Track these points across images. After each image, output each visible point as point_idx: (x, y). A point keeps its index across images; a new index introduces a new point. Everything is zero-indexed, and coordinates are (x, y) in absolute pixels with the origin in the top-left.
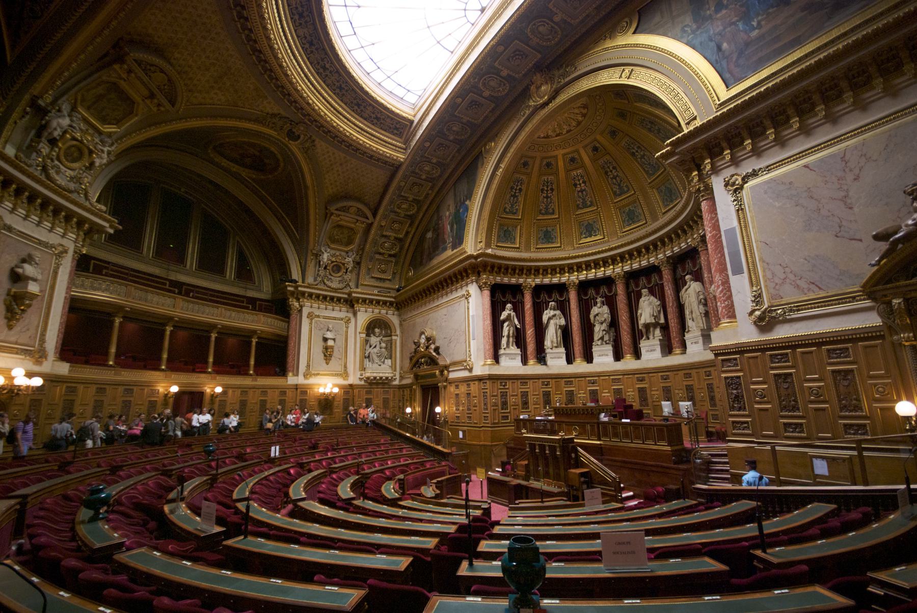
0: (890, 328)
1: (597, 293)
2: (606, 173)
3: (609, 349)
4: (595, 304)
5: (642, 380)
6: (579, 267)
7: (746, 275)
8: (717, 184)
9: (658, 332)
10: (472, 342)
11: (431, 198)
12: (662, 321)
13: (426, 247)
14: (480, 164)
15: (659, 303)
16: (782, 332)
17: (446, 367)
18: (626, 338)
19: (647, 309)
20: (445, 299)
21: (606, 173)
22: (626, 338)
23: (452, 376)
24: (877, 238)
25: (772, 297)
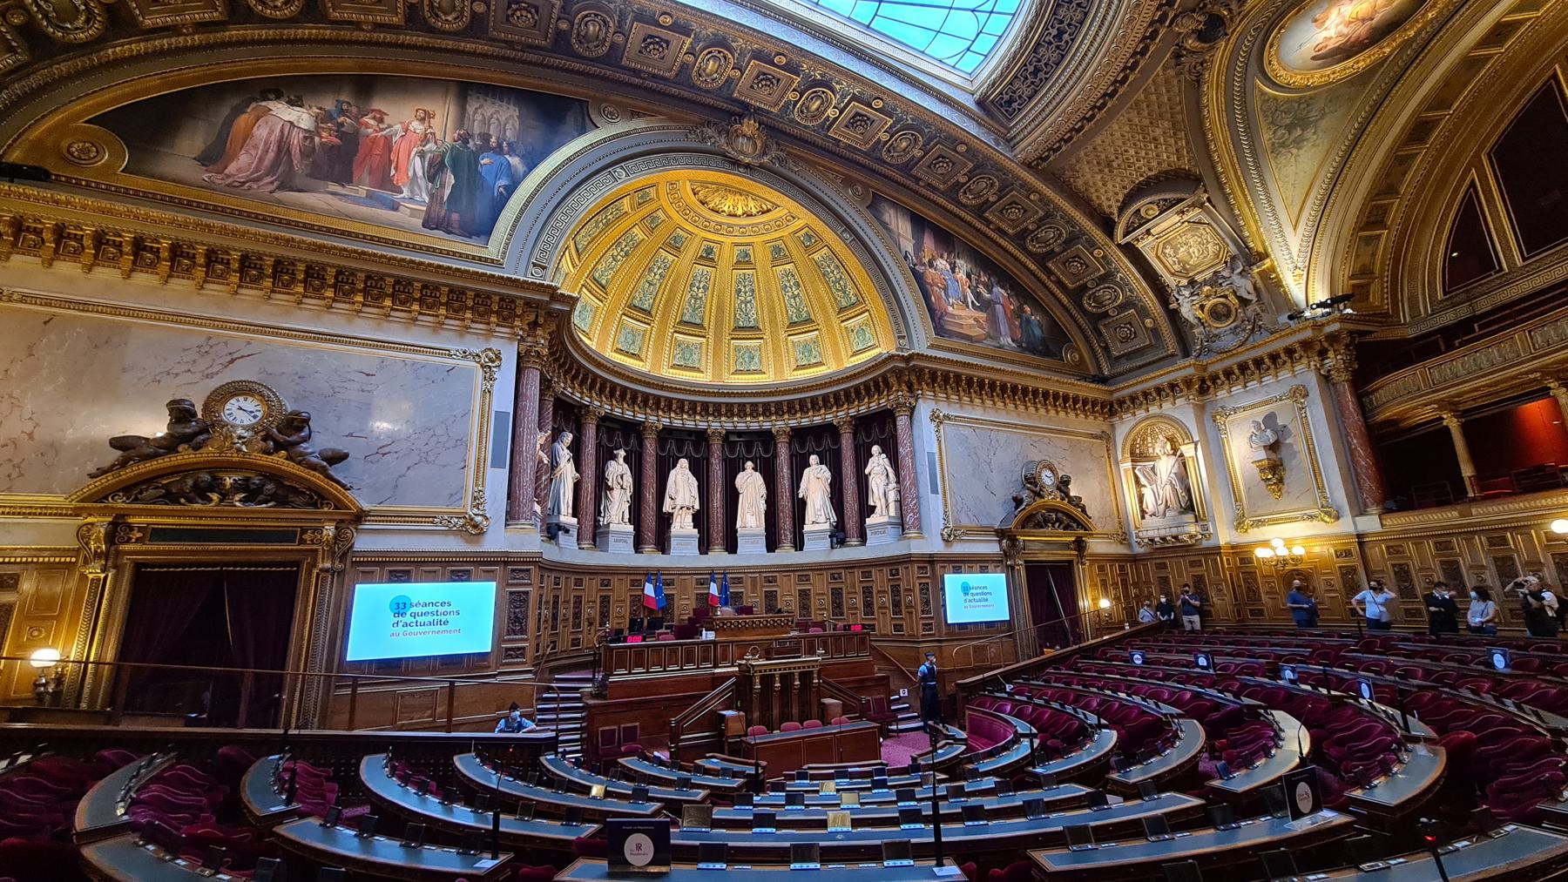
0: (1006, 555)
1: (610, 441)
2: (692, 285)
3: (631, 528)
4: (614, 457)
5: (669, 584)
6: (730, 411)
7: (940, 495)
8: (924, 408)
9: (689, 518)
10: (490, 471)
11: (345, 34)
12: (697, 507)
13: (261, 132)
14: (570, 119)
15: (696, 483)
16: (958, 549)
17: (360, 517)
18: (650, 519)
19: (682, 486)
20: (364, 328)
21: (692, 285)
22: (650, 519)
23: (364, 543)
24: (1015, 499)
25: (955, 520)
